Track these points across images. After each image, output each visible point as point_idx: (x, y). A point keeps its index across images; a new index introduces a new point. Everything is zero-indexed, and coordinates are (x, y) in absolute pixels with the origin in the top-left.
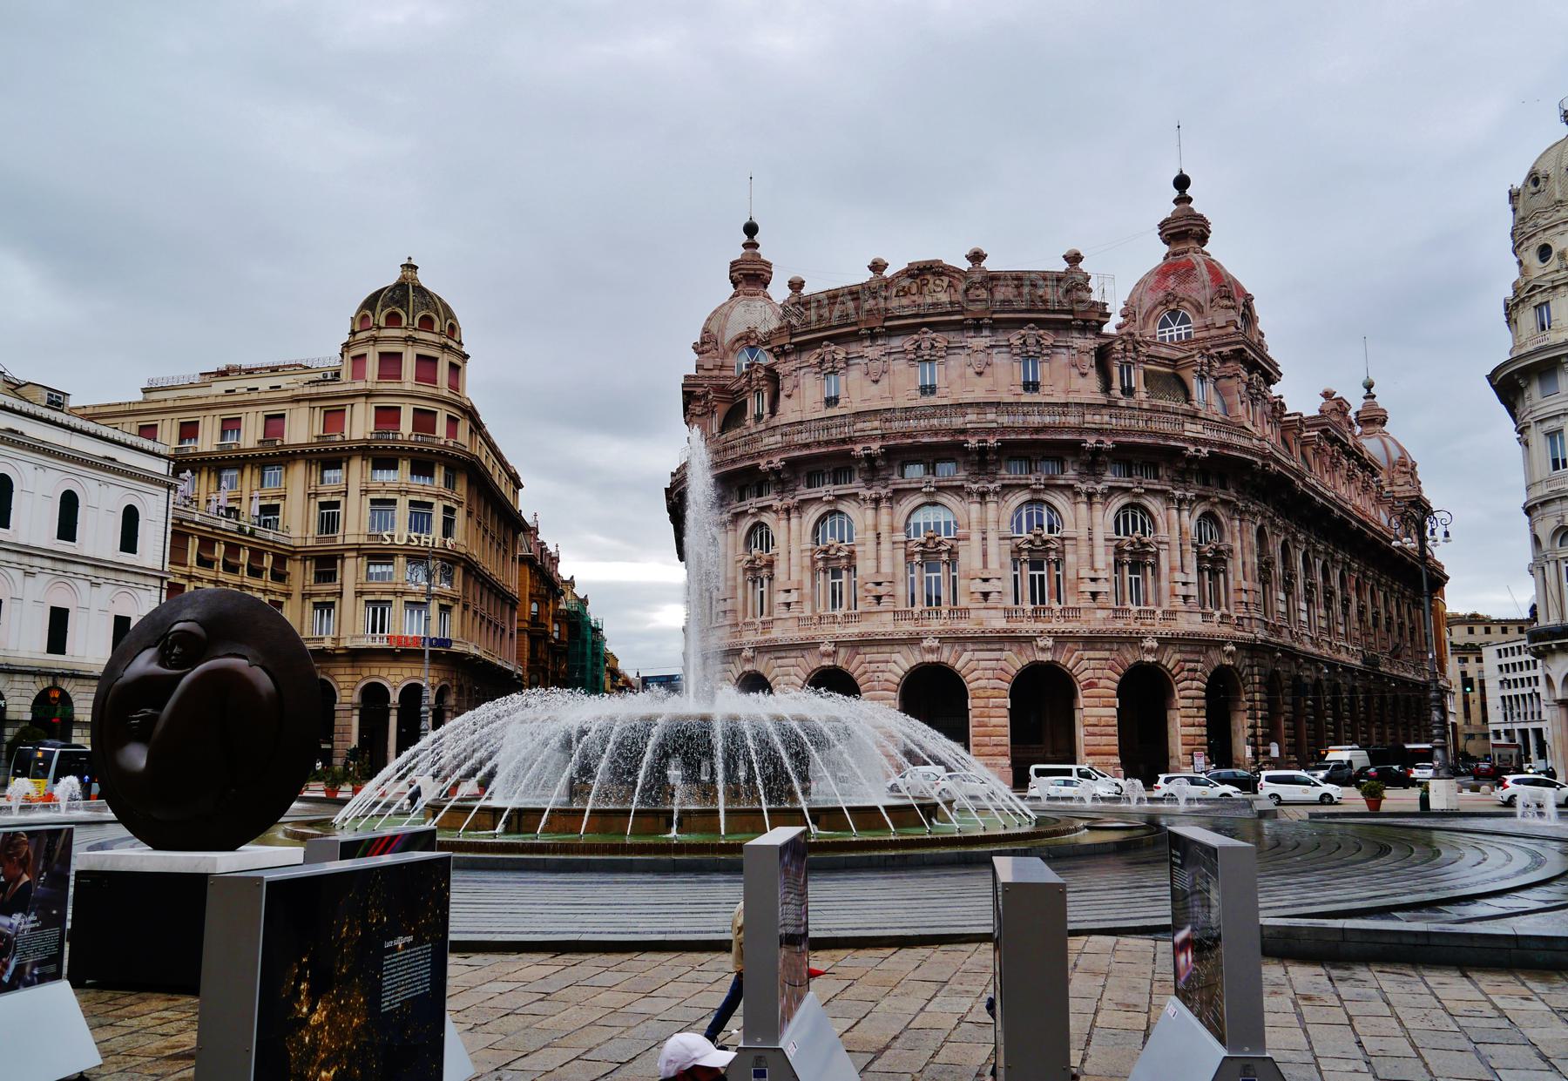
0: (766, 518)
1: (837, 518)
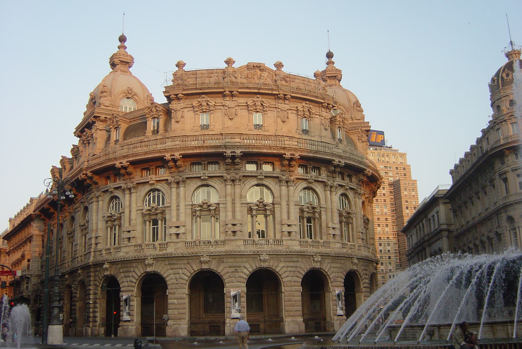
1: (206, 189)
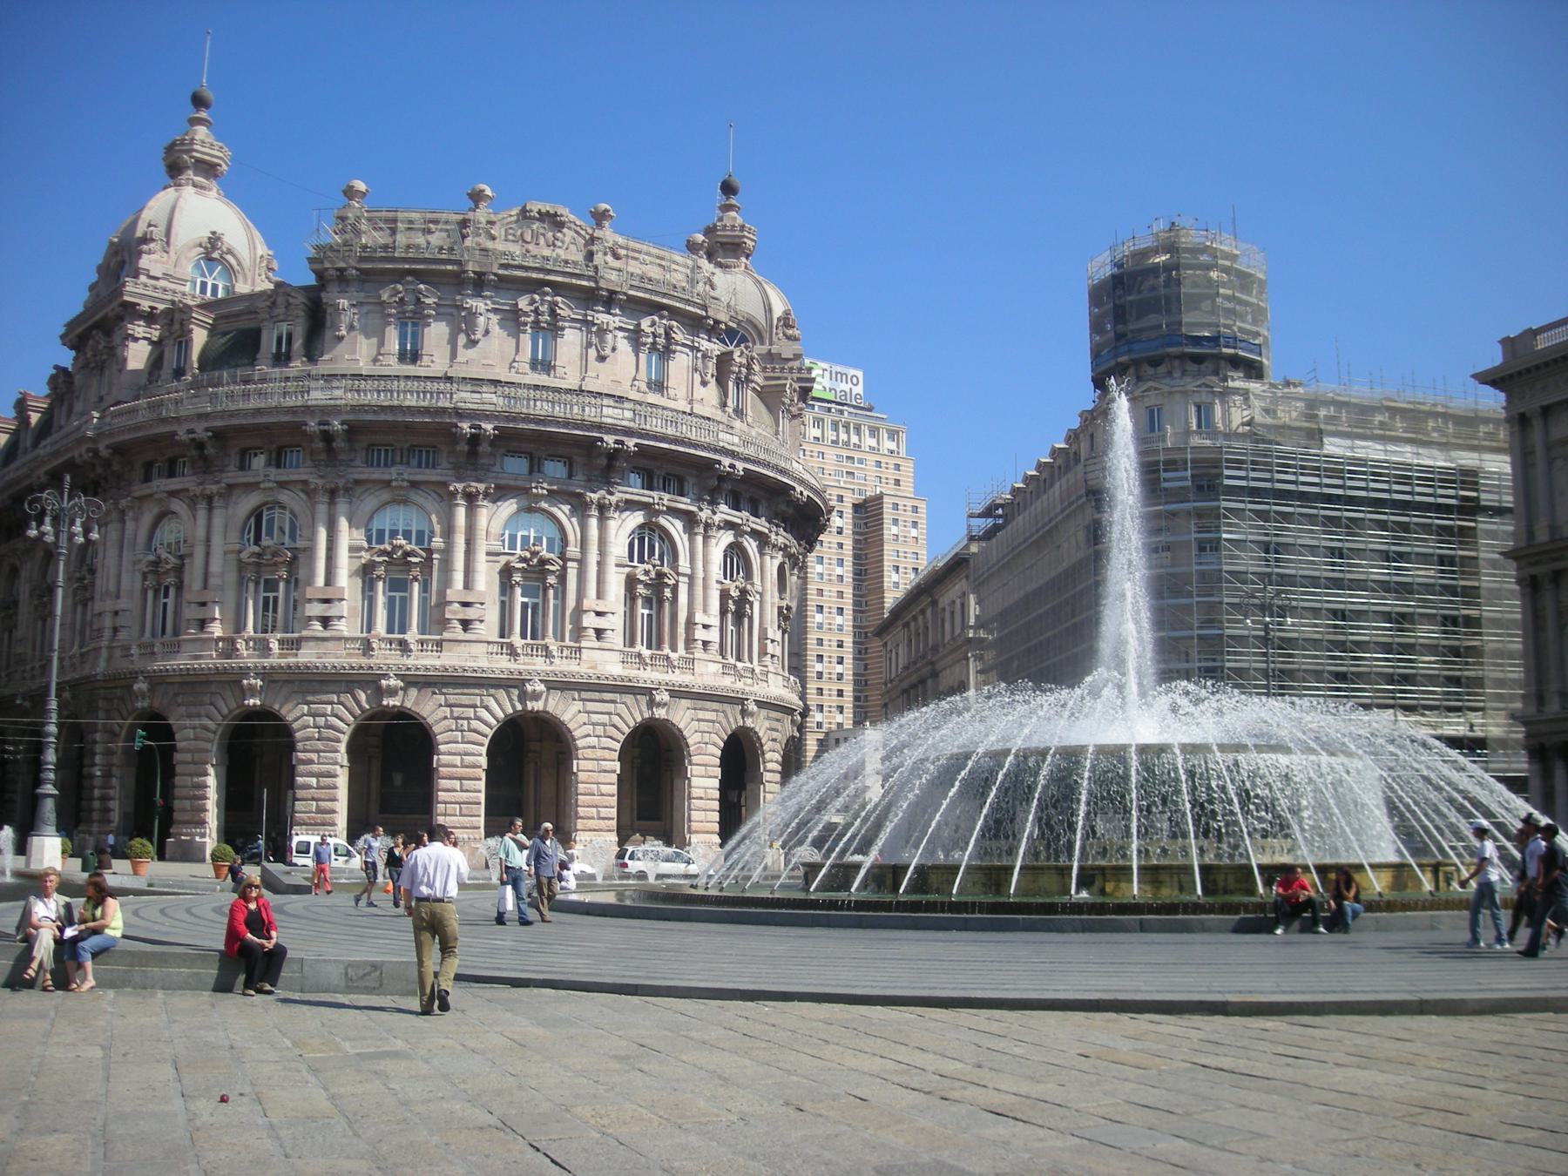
0: (284, 497)
